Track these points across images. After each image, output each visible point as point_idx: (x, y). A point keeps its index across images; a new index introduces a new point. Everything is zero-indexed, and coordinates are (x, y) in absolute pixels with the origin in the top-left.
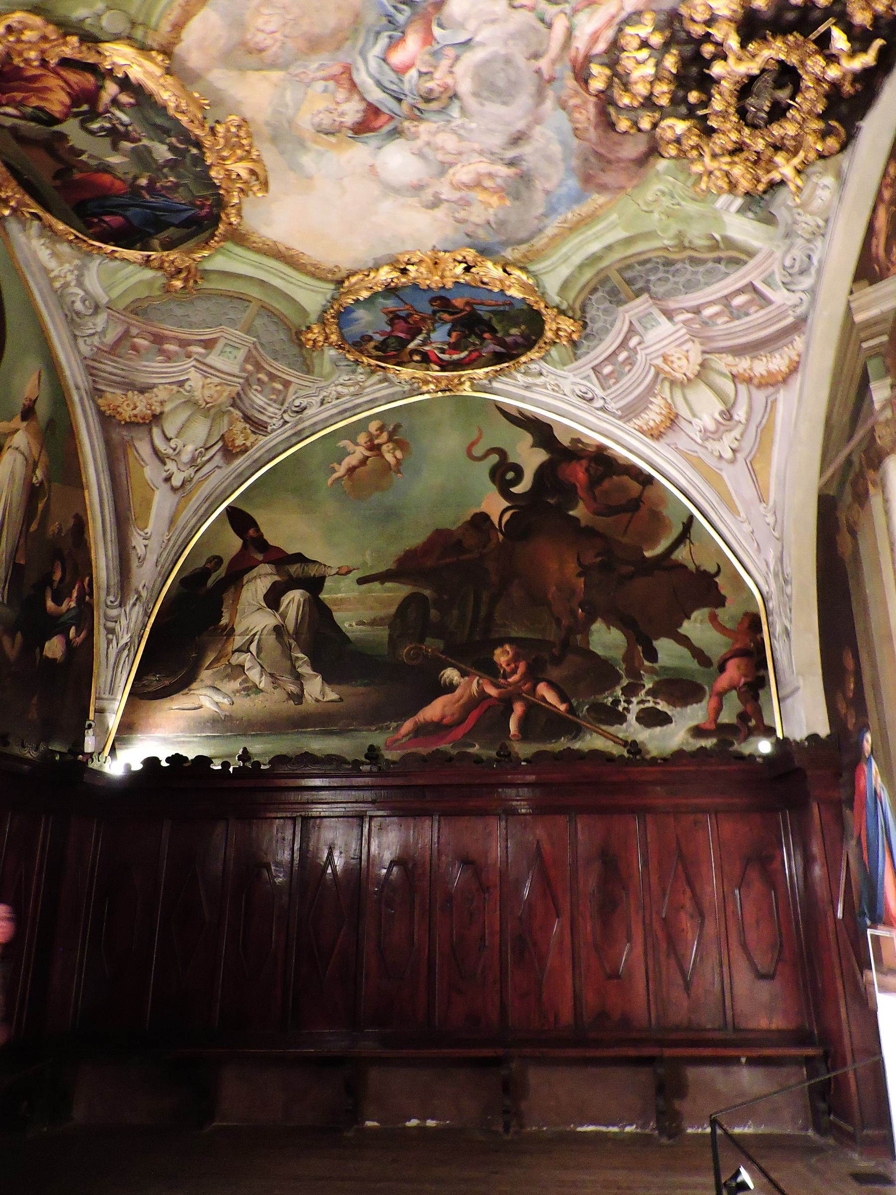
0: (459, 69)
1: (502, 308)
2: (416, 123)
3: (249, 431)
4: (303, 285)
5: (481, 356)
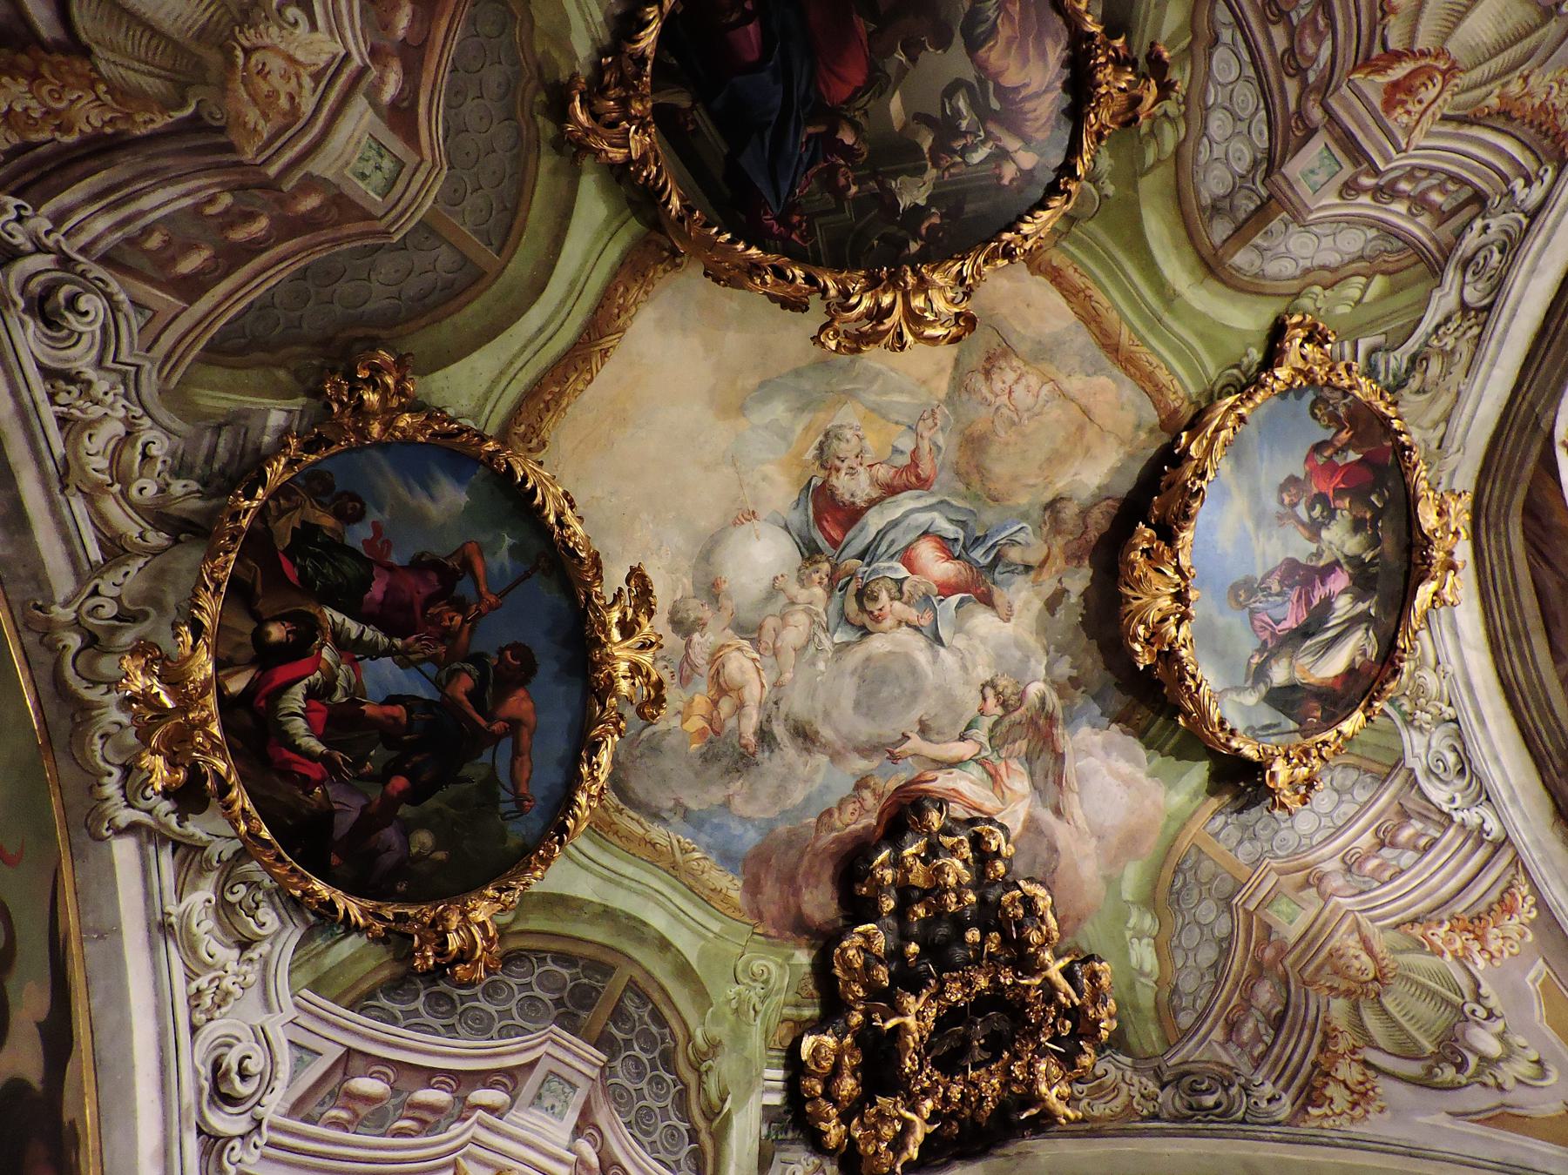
0: (904, 634)
1: (504, 795)
4: (512, 372)
5: (307, 784)
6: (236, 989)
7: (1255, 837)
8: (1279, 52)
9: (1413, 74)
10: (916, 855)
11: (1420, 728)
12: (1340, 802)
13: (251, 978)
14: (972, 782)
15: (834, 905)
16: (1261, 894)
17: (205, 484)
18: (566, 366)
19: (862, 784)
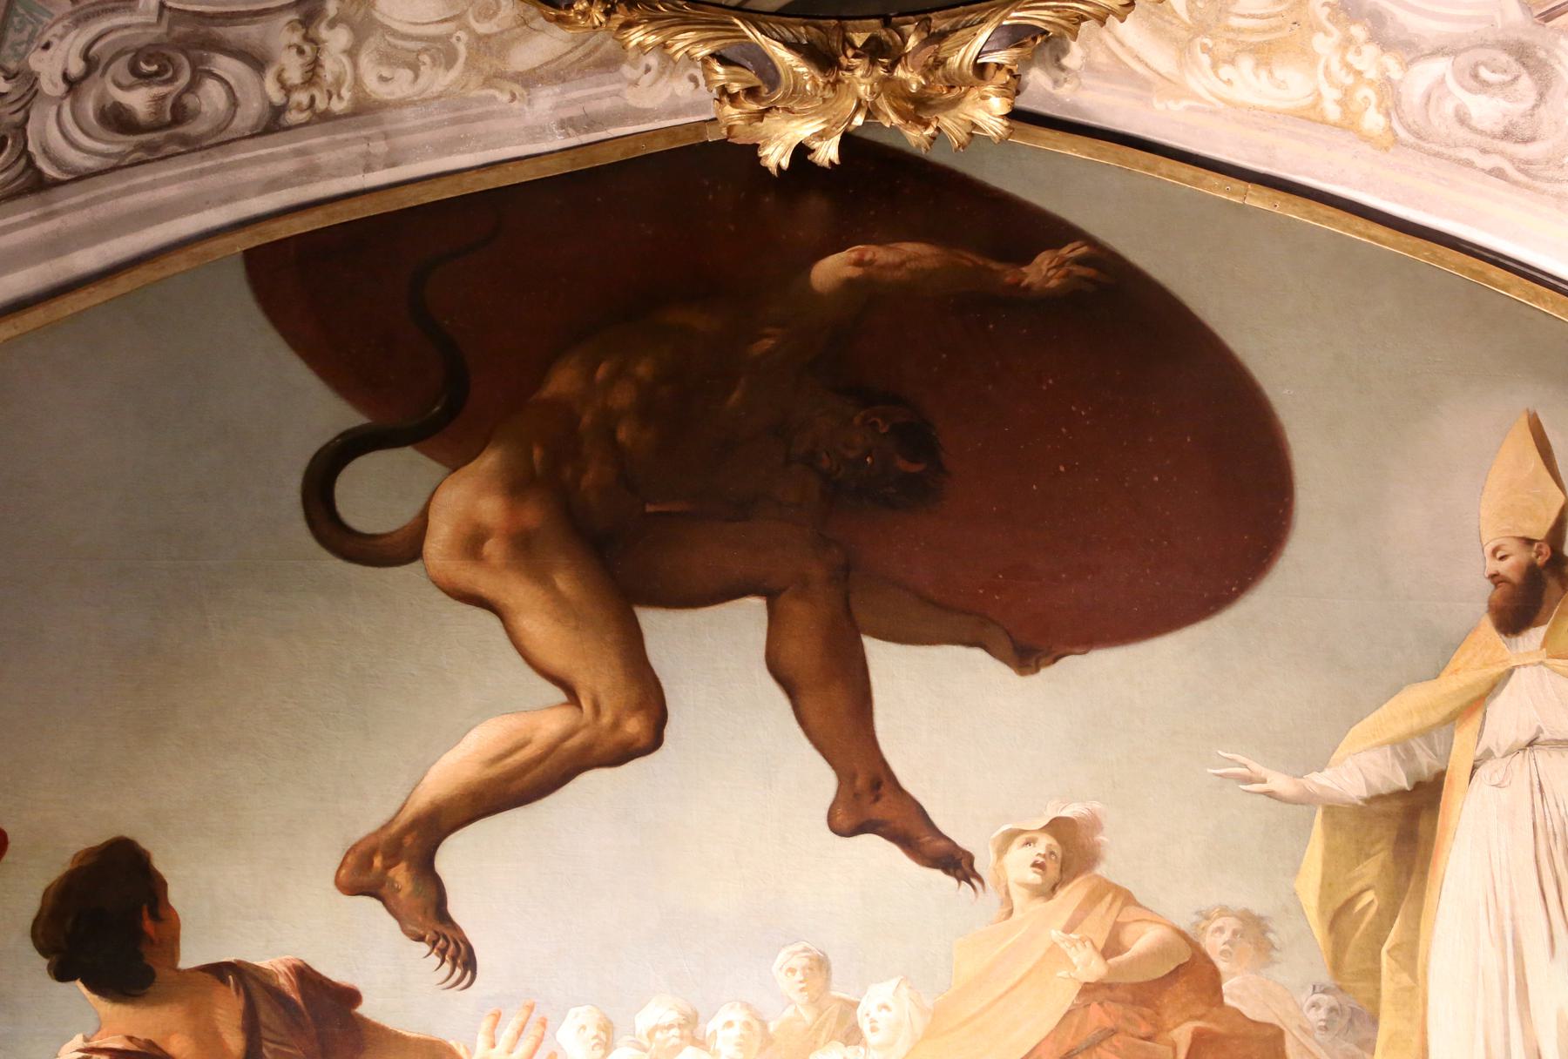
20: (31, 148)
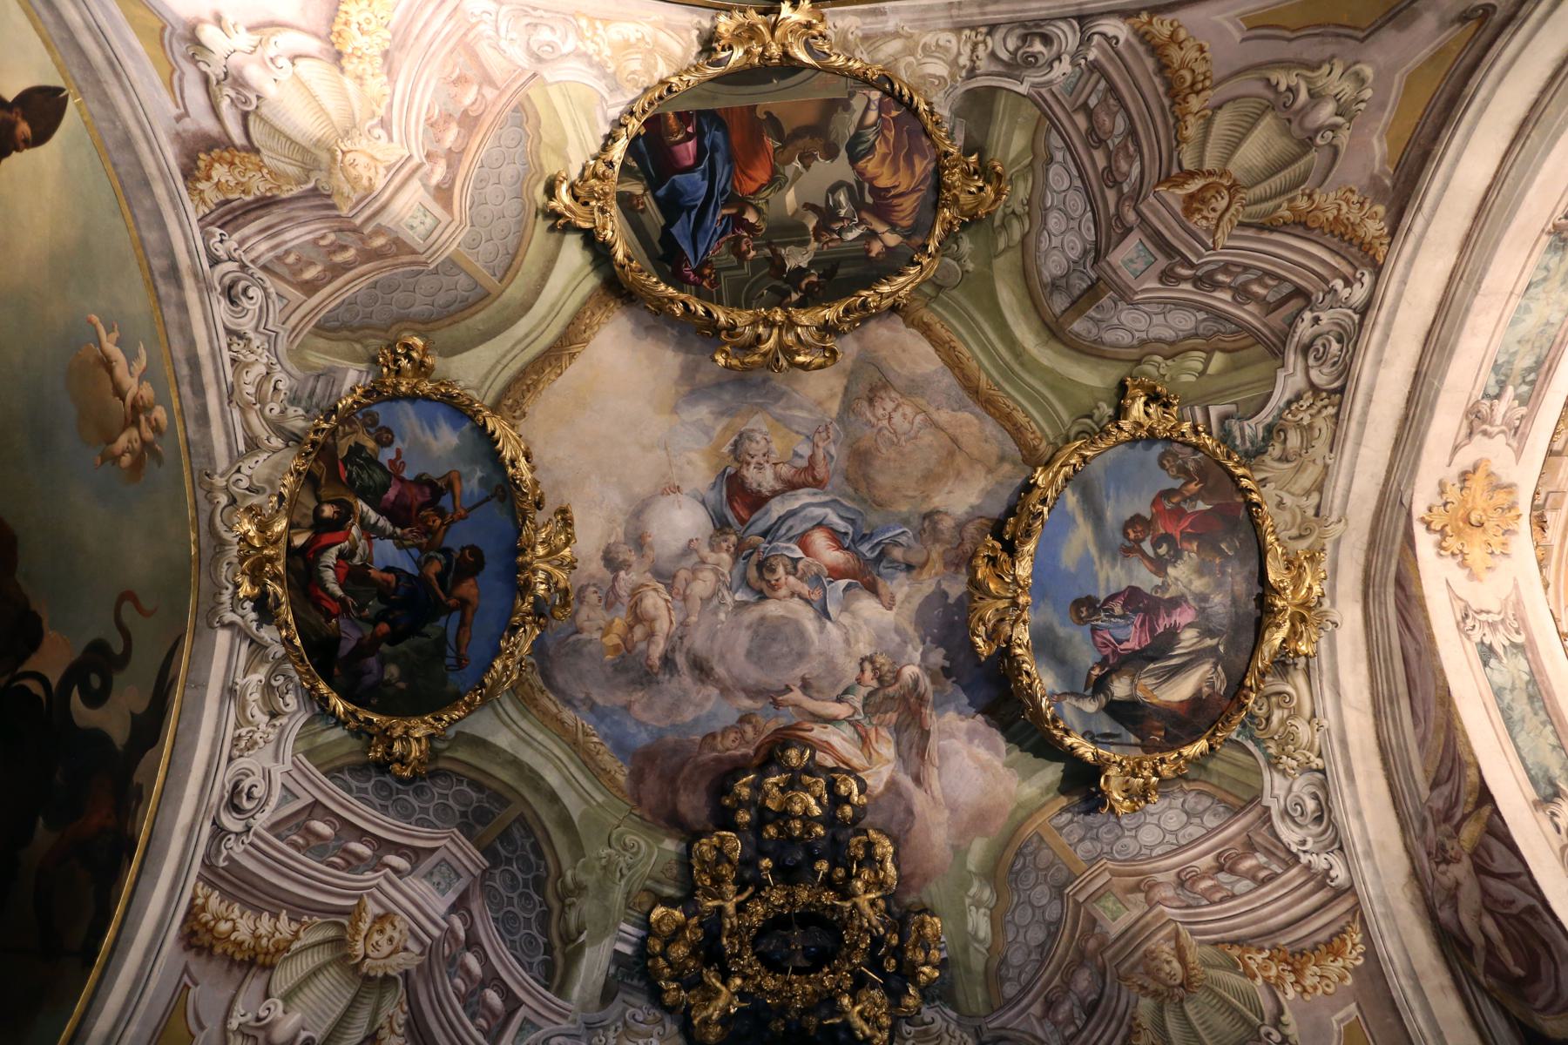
0: (796, 604)
1: (450, 652)
2: (732, 549)
3: (231, 196)
4: (505, 362)
5: (329, 616)
6: (261, 742)
7: (1097, 838)
8: (1100, 169)
9: (1202, 190)
10: (776, 784)
11: (1284, 773)
12: (1188, 823)
13: (271, 737)
14: (844, 739)
15: (707, 812)
16: (1092, 889)
17: (307, 412)
18: (544, 361)
19: (745, 718)
20: (1079, 34)
